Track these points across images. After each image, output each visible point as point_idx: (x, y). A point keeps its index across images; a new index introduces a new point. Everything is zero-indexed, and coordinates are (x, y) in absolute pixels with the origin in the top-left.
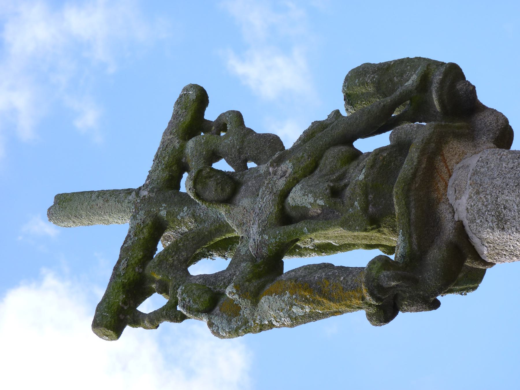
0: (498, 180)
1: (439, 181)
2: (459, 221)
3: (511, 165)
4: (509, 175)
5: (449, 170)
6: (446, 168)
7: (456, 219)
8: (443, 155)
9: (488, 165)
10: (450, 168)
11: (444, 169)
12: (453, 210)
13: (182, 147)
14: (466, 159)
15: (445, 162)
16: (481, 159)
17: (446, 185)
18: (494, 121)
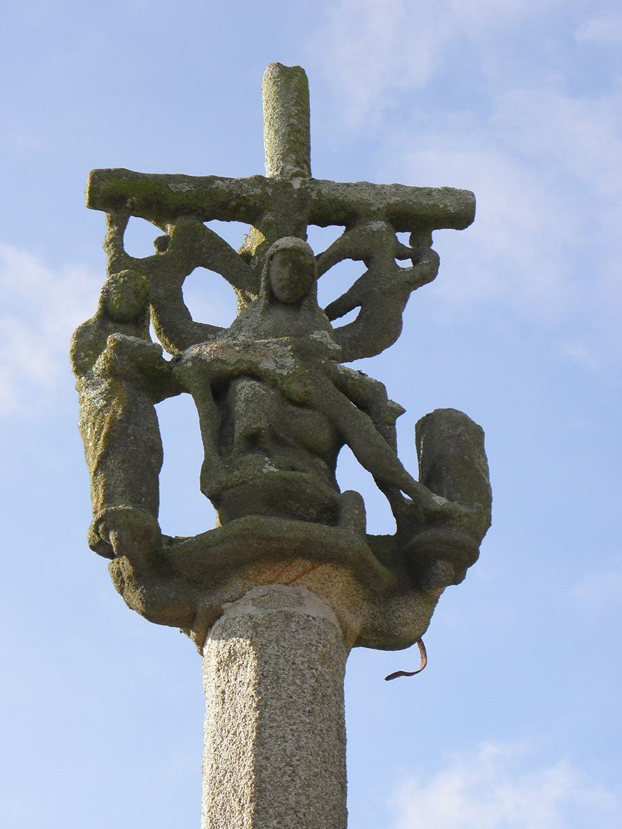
0: (274, 648)
1: (274, 571)
2: (222, 610)
3: (298, 661)
4: (282, 661)
5: (295, 580)
6: (297, 576)
7: (223, 607)
8: (314, 568)
9: (300, 631)
10: (298, 581)
11: (293, 574)
12: (237, 599)
13: (374, 216)
14: (319, 599)
15: (304, 573)
16: (311, 618)
17: (271, 582)
18: (402, 621)
